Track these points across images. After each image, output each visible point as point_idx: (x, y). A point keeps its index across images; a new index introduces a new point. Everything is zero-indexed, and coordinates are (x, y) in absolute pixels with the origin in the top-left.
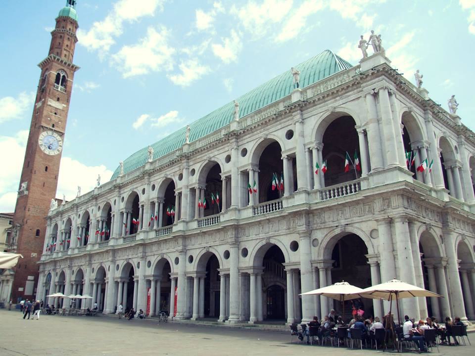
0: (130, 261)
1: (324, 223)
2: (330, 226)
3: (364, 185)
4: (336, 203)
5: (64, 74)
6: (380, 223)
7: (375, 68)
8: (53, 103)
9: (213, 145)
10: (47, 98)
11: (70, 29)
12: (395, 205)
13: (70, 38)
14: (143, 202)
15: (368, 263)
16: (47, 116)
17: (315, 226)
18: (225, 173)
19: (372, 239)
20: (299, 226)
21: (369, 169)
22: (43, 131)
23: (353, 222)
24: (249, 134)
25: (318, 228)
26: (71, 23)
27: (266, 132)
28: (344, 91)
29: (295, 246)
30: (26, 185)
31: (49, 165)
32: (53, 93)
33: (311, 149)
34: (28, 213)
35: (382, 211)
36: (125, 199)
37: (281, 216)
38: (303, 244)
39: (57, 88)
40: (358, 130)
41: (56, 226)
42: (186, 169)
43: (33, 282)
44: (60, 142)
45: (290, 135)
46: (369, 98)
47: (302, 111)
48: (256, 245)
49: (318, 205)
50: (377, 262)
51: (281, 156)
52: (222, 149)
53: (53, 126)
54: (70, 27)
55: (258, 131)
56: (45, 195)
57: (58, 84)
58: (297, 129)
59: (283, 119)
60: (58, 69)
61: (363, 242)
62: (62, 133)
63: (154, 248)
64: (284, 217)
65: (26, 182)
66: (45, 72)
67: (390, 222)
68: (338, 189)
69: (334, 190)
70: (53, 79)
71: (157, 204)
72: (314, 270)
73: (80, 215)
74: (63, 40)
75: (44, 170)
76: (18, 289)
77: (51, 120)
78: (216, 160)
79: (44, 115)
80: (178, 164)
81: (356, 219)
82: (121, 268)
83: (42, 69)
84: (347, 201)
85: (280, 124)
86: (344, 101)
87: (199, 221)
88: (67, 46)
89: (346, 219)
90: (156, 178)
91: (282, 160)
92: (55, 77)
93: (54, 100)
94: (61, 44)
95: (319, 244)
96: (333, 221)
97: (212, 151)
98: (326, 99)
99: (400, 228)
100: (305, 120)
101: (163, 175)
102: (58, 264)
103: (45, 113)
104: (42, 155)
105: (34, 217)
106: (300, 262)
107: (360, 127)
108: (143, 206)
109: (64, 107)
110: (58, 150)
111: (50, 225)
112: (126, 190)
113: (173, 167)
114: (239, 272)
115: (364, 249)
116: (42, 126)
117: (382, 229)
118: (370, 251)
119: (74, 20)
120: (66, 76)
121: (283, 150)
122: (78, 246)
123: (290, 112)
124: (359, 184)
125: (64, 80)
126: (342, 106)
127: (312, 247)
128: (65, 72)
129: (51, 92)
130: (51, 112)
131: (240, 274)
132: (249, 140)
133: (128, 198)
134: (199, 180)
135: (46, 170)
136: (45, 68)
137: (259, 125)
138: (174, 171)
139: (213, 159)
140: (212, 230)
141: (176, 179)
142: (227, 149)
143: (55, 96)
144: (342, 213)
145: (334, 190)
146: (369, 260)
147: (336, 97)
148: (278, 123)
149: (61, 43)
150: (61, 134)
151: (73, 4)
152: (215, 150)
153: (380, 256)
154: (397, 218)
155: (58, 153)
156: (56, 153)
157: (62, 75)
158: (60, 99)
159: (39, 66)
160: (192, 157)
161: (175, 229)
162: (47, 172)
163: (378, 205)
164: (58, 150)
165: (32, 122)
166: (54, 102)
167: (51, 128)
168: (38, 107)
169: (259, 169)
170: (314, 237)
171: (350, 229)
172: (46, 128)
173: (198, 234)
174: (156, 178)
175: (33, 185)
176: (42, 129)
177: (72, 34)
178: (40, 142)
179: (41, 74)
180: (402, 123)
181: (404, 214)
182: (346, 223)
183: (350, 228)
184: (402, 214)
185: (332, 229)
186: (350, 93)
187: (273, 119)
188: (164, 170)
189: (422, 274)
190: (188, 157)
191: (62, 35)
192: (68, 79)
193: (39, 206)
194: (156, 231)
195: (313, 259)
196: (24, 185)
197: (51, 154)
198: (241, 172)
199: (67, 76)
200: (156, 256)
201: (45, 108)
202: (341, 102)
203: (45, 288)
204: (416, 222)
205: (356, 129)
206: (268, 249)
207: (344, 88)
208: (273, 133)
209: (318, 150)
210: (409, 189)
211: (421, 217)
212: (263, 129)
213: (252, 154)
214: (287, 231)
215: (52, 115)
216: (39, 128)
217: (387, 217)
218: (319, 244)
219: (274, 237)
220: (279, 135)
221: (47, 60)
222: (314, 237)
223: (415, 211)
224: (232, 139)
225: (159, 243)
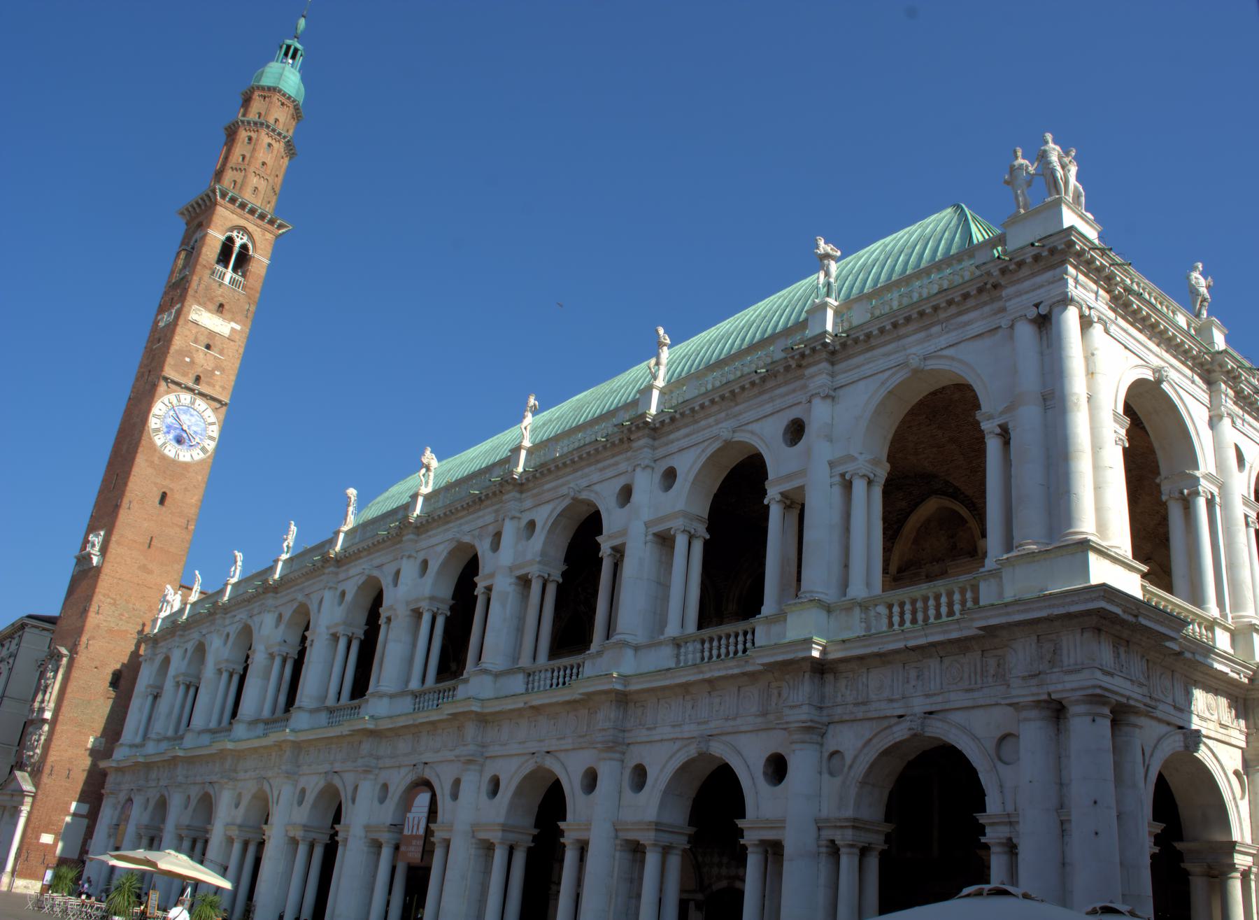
0: (337, 781)
1: (864, 703)
2: (882, 714)
3: (987, 594)
4: (901, 645)
5: (245, 239)
6: (1025, 714)
7: (1045, 242)
8: (202, 317)
9: (588, 453)
10: (189, 299)
11: (277, 120)
12: (1072, 661)
13: (276, 145)
14: (391, 608)
15: (983, 840)
16: (182, 353)
17: (839, 710)
18: (610, 537)
19: (999, 765)
20: (792, 707)
21: (1009, 545)
22: (168, 393)
23: (947, 706)
24: (686, 426)
25: (846, 717)
26: (283, 104)
27: (731, 423)
28: (953, 309)
29: (777, 768)
30: (101, 538)
31: (172, 490)
32: (208, 288)
33: (847, 477)
34: (93, 619)
35: (1032, 676)
36: (349, 597)
37: (744, 674)
38: (801, 764)
39: (222, 276)
40: (985, 426)
41: (167, 661)
42: (513, 518)
43: (85, 821)
44: (211, 427)
45: (796, 431)
46: (1026, 332)
47: (833, 364)
48: (671, 757)
49: (847, 645)
50: (1010, 839)
51: (765, 492)
52: (610, 466)
53: (198, 379)
54: (276, 116)
55: (711, 420)
56: (150, 572)
57: (226, 267)
58: (819, 415)
59: (779, 386)
60: (229, 225)
61: (972, 773)
62: (219, 401)
63: (403, 746)
64: (752, 676)
65: (102, 533)
66: (194, 232)
67: (1057, 711)
68: (913, 602)
69: (902, 605)
70: (211, 250)
71: (426, 618)
72: (824, 850)
73: (228, 635)
74: (254, 150)
75: (157, 500)
76: (38, 838)
77: (192, 362)
78: (592, 497)
79: (173, 349)
80: (493, 505)
81: (958, 699)
82: (310, 797)
83: (187, 224)
84: (932, 639)
85: (772, 400)
86: (952, 337)
87: (529, 675)
88: (264, 164)
89: (927, 696)
90: (433, 541)
91: (768, 507)
92: (217, 248)
93: (210, 311)
94: (247, 159)
95: (846, 769)
96: (891, 701)
97: (586, 470)
98: (902, 331)
99: (1089, 732)
100: (841, 392)
101: (450, 535)
102: (154, 775)
103: (178, 342)
104: (156, 460)
105: (110, 631)
106: (784, 821)
107: (990, 417)
108: (389, 619)
110: (204, 450)
111: (152, 660)
112: (352, 572)
113: (481, 513)
114: (616, 837)
115: (977, 798)
116: (166, 379)
117: (1033, 733)
118: (993, 804)
119: (289, 98)
120: (250, 246)
121: (771, 475)
122: (213, 725)
123: (799, 366)
124: (975, 589)
125: (243, 259)
126: (945, 352)
127: (826, 776)
128: (251, 237)
129: (202, 286)
130: (196, 341)
131: (618, 842)
132: (684, 443)
133: (356, 595)
134: (543, 553)
135: (162, 501)
136: (196, 222)
137: (713, 402)
138: (480, 523)
139: (584, 495)
140: (557, 704)
141: (483, 548)
142: (623, 467)
143: (211, 299)
144: (918, 677)
145: (902, 605)
146: (988, 830)
147: (933, 325)
148: (766, 397)
149: (248, 156)
150: (218, 405)
151: (293, 57)
152: (593, 468)
153: (1018, 822)
154: (1077, 702)
155: (202, 456)
156: (197, 458)
157: (238, 243)
158: (226, 307)
159: (182, 214)
160: (531, 485)
161: (462, 691)
162: (164, 509)
163: (1022, 655)
164: (204, 450)
165: (141, 367)
167: (191, 384)
168: (161, 324)
169: (708, 530)
170: (831, 744)
171: (941, 730)
172: (178, 384)
173: (519, 712)
174: (433, 541)
175: (118, 543)
176: (162, 386)
177: (279, 134)
178: (153, 423)
179: (184, 239)
180: (1128, 410)
181: (1098, 691)
182: (929, 709)
183: (939, 724)
184: (1090, 692)
185: (886, 723)
186: (972, 315)
187: (753, 384)
188: (457, 519)
189: (1150, 893)
190: (522, 484)
191: (254, 135)
192: (256, 256)
193: (127, 602)
194: (415, 695)
195: (825, 813)
196: (96, 540)
197: (181, 459)
198: (655, 534)
199: (254, 246)
200: (403, 771)
201: (179, 329)
202: (943, 341)
203: (112, 840)
204: (1143, 721)
205: (978, 423)
206: (708, 772)
207: (953, 299)
208: (750, 427)
209: (870, 482)
210: (1118, 611)
211: (1172, 711)
212: (723, 415)
213: (688, 485)
214: (760, 720)
215: (197, 350)
216: (154, 387)
217: (1045, 697)
218: (846, 769)
219: (724, 738)
220: (765, 435)
221: (202, 199)
222: (831, 744)
223: (1141, 685)
224: (639, 439)
225: (414, 731)
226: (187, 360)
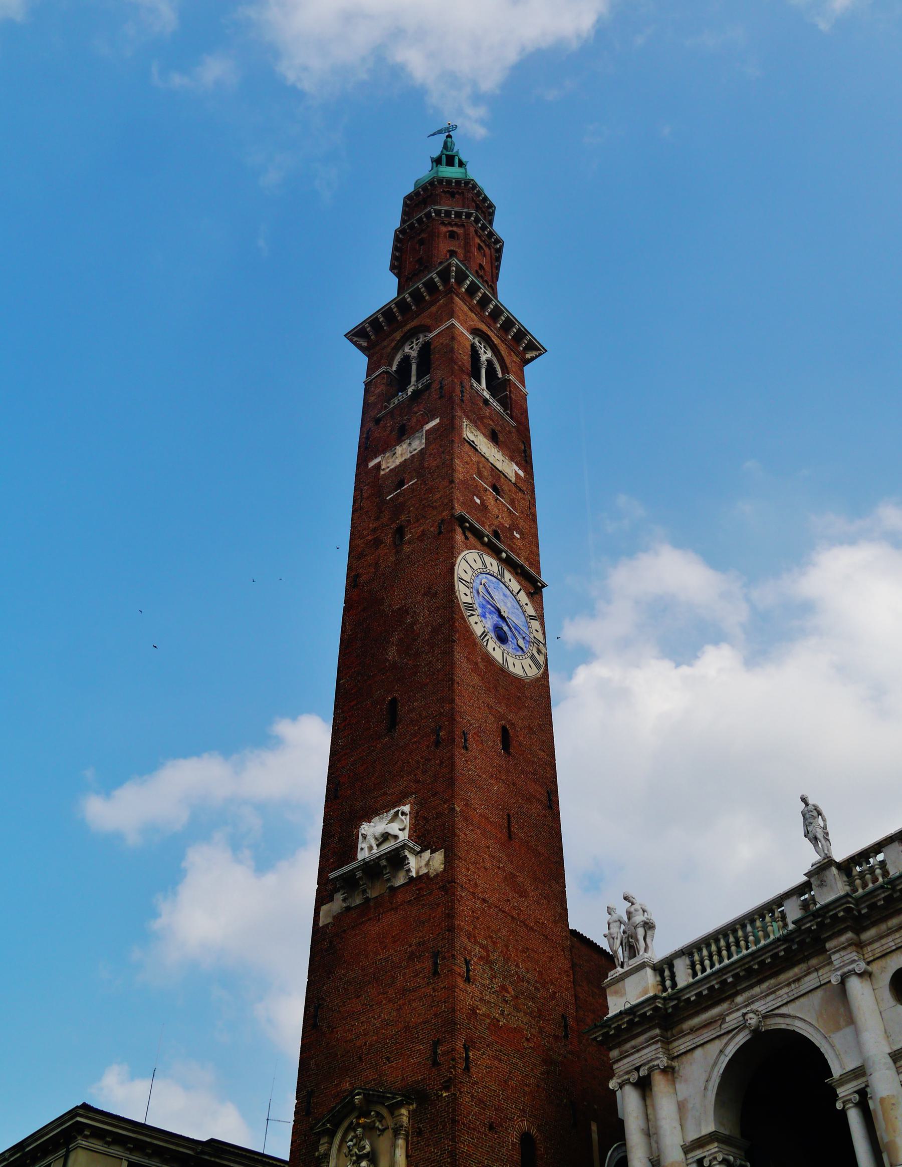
30: (407, 820)
56: (523, 894)
65: (407, 808)
109: (516, 474)
157: (484, 358)
159: (358, 335)
166: (485, 440)
215: (486, 490)
226: (478, 501)
